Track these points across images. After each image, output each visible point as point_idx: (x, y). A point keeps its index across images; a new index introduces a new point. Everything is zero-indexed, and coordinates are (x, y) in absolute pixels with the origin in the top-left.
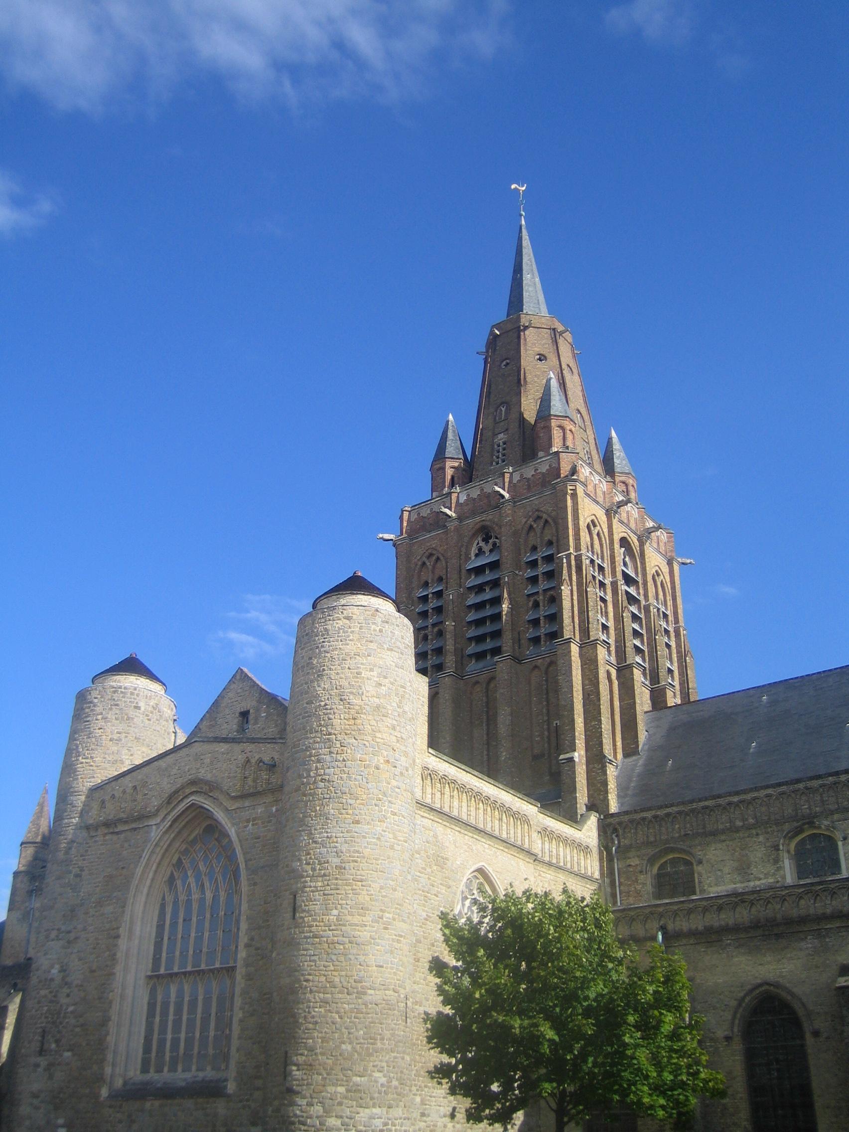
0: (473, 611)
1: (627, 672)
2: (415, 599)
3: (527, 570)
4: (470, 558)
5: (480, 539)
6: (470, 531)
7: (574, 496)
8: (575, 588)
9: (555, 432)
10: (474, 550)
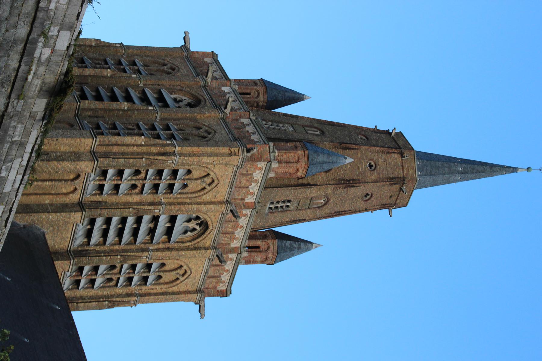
0: (124, 95)
1: (78, 208)
2: (133, 59)
3: (161, 125)
4: (171, 94)
5: (190, 101)
6: (195, 92)
7: (230, 154)
8: (144, 149)
9: (292, 154)
10: (178, 96)
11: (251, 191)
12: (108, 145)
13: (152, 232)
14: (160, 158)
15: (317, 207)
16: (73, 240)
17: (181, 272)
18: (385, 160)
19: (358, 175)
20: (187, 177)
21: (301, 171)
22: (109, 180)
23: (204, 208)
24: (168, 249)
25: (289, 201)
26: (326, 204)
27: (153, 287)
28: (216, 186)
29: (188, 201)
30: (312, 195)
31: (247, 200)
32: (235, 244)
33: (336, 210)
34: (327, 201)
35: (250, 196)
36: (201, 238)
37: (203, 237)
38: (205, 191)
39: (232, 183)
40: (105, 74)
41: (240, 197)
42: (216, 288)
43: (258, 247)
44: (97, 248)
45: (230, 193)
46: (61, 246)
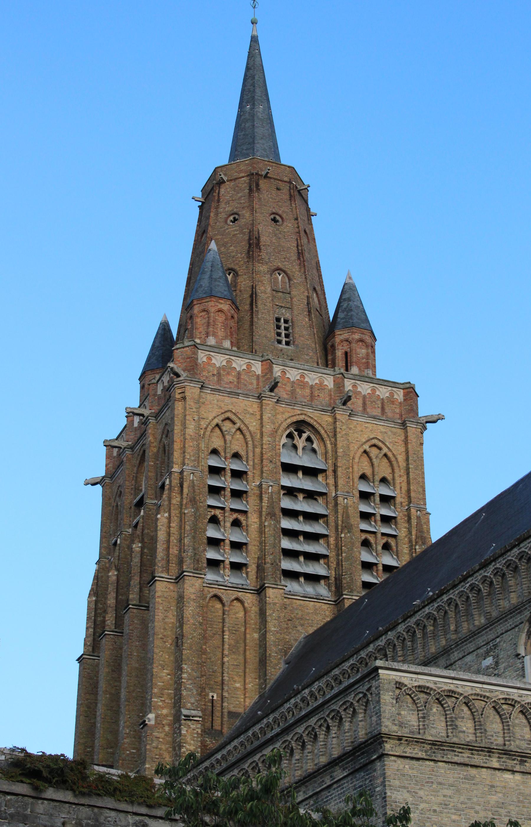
8: (175, 512)
11: (244, 367)
12: (168, 561)
13: (310, 495)
14: (185, 491)
15: (289, 282)
16: (318, 598)
17: (374, 452)
18: (228, 203)
19: (244, 234)
20: (222, 454)
21: (221, 306)
22: (223, 556)
23: (268, 428)
24: (335, 471)
25: (278, 320)
26: (285, 272)
27: (398, 487)
28: (235, 414)
29: (258, 450)
30: (269, 290)
31: (259, 372)
32: (329, 382)
33: (294, 257)
34: (279, 270)
35: (253, 369)
36: (320, 429)
37: (317, 426)
38: (244, 428)
39: (230, 393)
40: (114, 578)
41: (255, 382)
42: (400, 403)
43: (346, 353)
44: (333, 565)
45: (247, 395)
46: (327, 613)
